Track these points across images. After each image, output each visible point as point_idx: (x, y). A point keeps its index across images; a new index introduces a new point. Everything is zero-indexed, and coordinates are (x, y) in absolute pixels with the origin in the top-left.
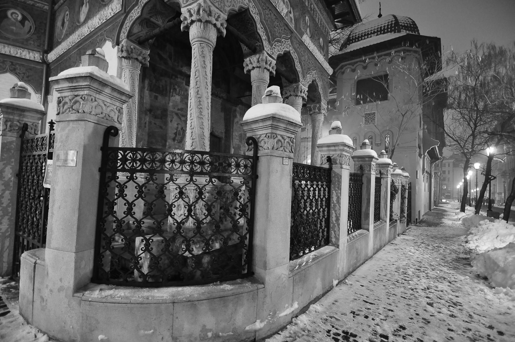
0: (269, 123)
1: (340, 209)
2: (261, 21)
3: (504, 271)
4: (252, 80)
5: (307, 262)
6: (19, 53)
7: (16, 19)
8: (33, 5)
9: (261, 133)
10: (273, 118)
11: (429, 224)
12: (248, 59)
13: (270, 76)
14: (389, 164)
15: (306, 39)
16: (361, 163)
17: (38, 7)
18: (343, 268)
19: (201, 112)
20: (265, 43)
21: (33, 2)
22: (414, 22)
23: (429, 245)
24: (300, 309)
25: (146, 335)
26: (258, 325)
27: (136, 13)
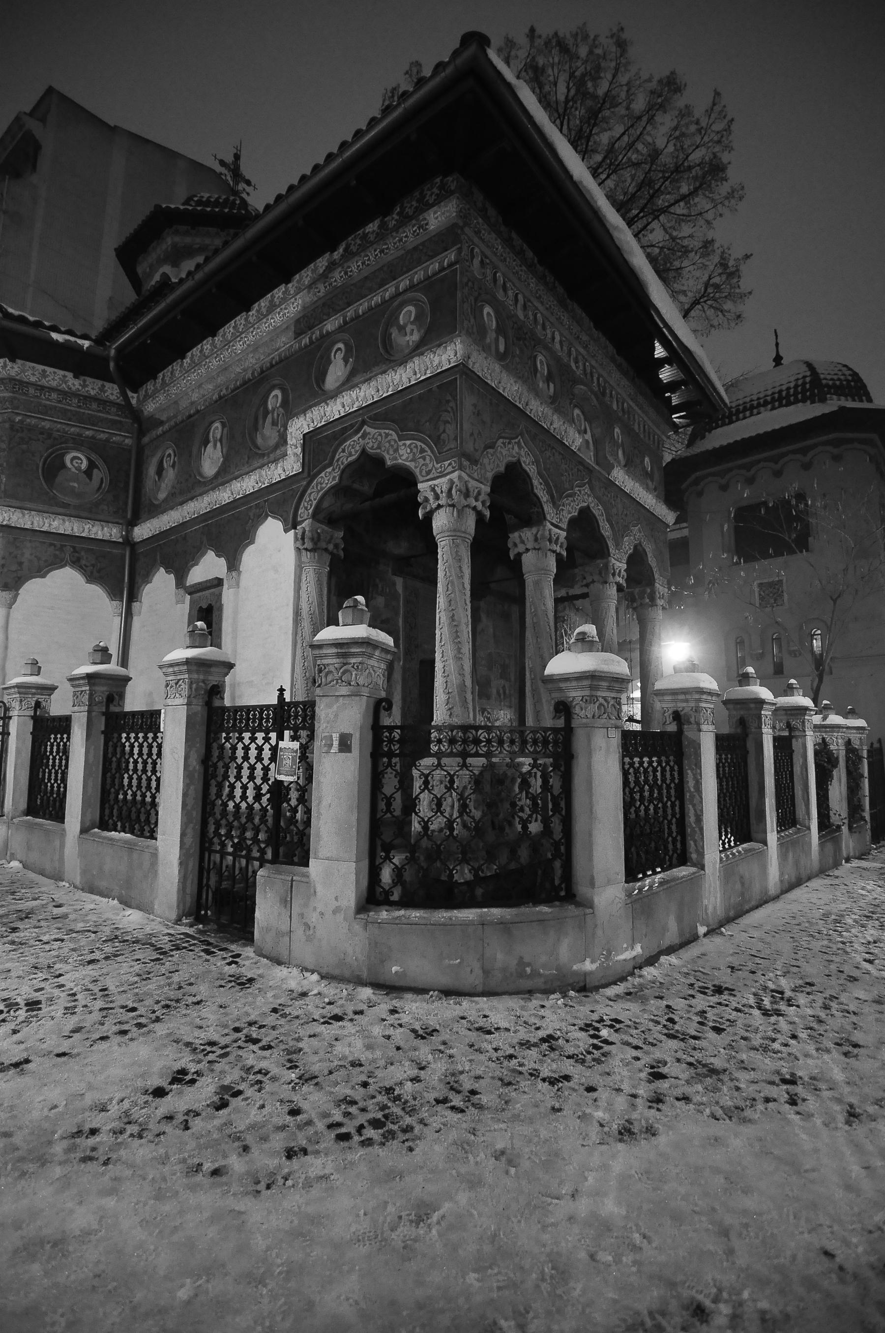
0: (586, 683)
1: (701, 802)
2: (539, 473)
4: (524, 570)
5: (651, 887)
6: (86, 530)
8: (107, 440)
9: (575, 694)
10: (592, 678)
12: (516, 534)
13: (557, 561)
14: (806, 709)
15: (619, 476)
17: (114, 442)
18: (715, 908)
19: (459, 650)
20: (548, 508)
21: (107, 436)
22: (855, 375)
24: (644, 957)
26: (588, 966)
27: (328, 479)
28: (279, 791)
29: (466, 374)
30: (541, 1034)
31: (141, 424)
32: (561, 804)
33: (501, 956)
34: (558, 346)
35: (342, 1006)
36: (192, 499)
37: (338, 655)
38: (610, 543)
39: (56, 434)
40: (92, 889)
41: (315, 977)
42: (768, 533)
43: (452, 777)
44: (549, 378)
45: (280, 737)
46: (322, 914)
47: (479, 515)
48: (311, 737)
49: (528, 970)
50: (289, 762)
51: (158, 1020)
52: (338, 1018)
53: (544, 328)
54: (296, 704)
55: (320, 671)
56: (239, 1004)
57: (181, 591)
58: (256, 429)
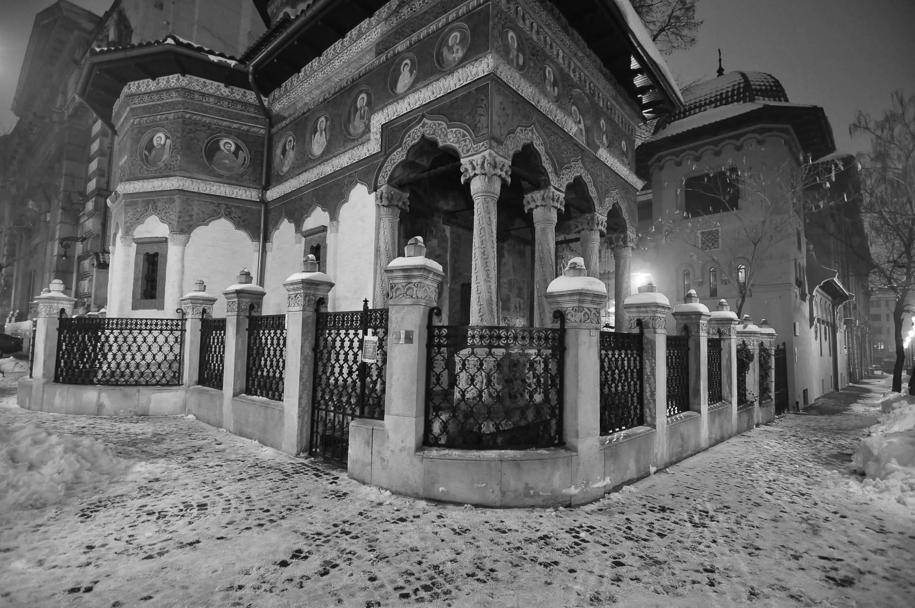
2: (546, 152)
3: (877, 460)
5: (618, 439)
7: (229, 151)
8: (248, 131)
9: (568, 306)
11: (820, 410)
12: (529, 195)
13: (558, 214)
15: (603, 154)
16: (686, 321)
19: (488, 275)
20: (552, 176)
22: (777, 81)
23: (802, 439)
25: (479, 488)
26: (573, 491)
27: (399, 156)
28: (364, 369)
29: (496, 81)
30: (540, 534)
31: (271, 119)
32: (556, 382)
33: (513, 482)
34: (561, 61)
35: (406, 512)
36: (305, 171)
37: (405, 277)
38: (596, 202)
39: (213, 127)
40: (241, 434)
41: (388, 493)
42: (710, 196)
43: (481, 361)
44: (555, 84)
45: (365, 333)
46: (392, 451)
47: (503, 180)
48: (386, 333)
49: (532, 492)
50: (371, 350)
51: (283, 518)
52: (402, 520)
53: (551, 47)
54: (375, 311)
55: (392, 288)
56: (337, 509)
57: (299, 235)
58: (349, 122)
